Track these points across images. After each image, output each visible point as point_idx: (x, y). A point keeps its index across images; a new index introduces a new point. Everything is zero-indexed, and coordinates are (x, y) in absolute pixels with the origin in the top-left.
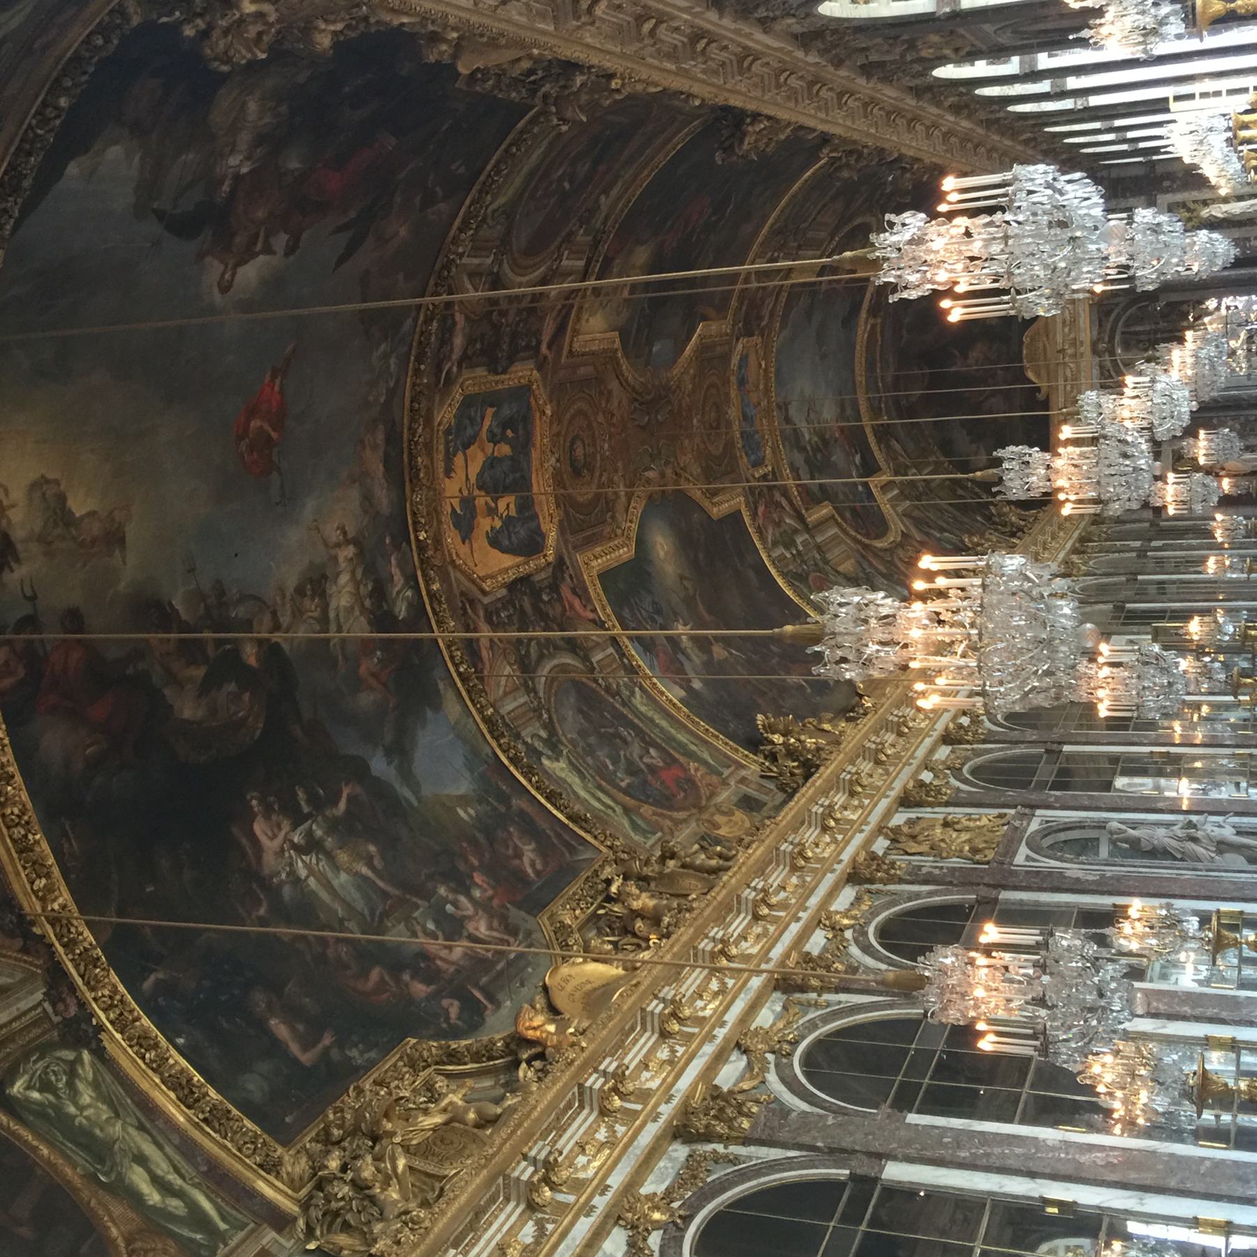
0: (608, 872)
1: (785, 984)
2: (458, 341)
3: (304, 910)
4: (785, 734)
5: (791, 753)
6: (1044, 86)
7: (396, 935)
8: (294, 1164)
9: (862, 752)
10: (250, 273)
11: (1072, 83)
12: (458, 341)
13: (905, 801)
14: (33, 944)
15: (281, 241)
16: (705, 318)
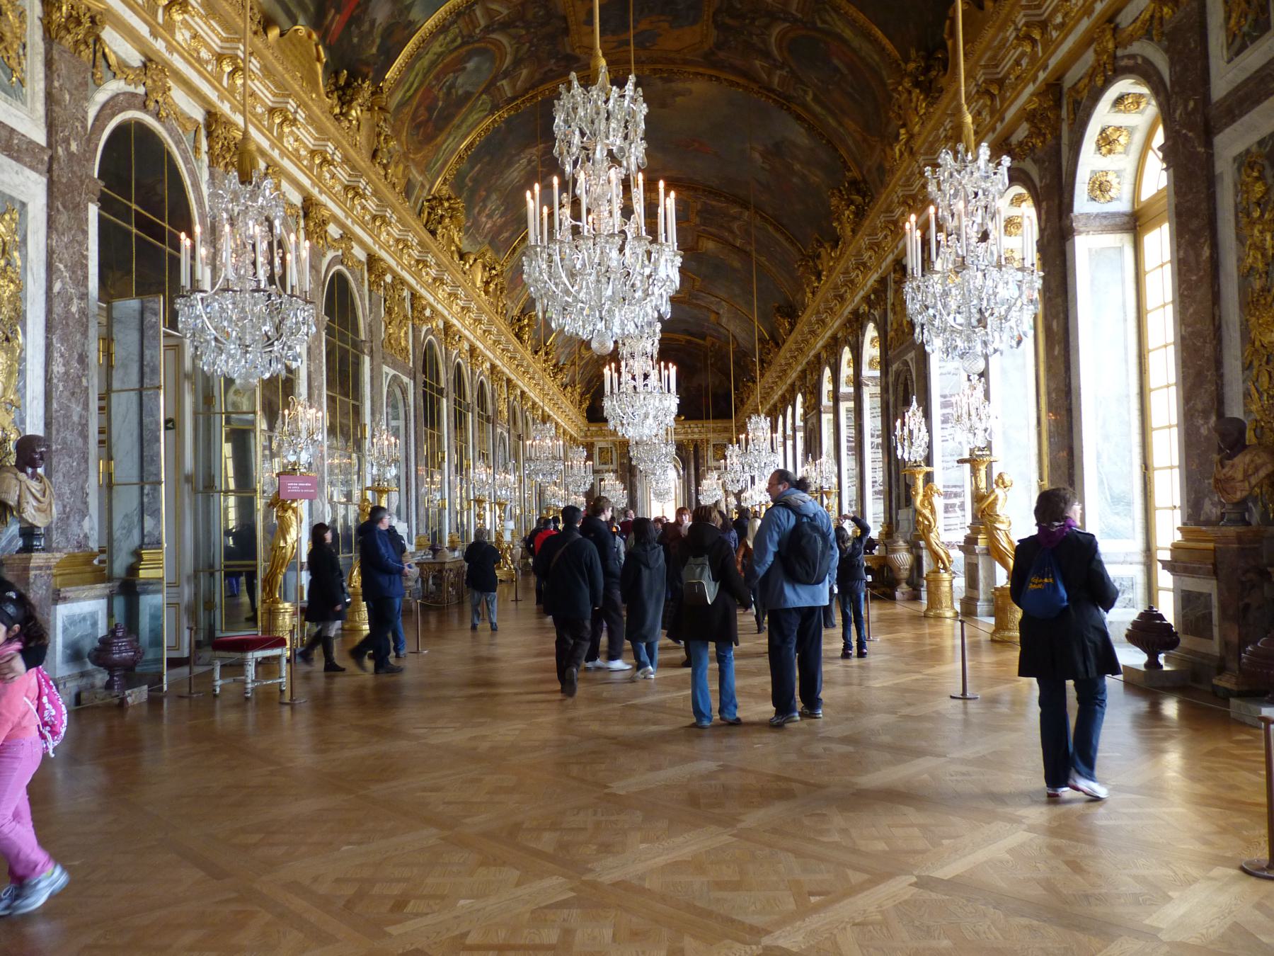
0: (498, 268)
1: (472, 350)
2: (714, 203)
3: (510, 164)
4: (528, 325)
5: (521, 328)
6: (789, 432)
7: (494, 197)
8: (445, 191)
9: (523, 359)
10: (756, 155)
11: (789, 443)
12: (714, 203)
13: (509, 381)
14: (526, 91)
15: (768, 167)
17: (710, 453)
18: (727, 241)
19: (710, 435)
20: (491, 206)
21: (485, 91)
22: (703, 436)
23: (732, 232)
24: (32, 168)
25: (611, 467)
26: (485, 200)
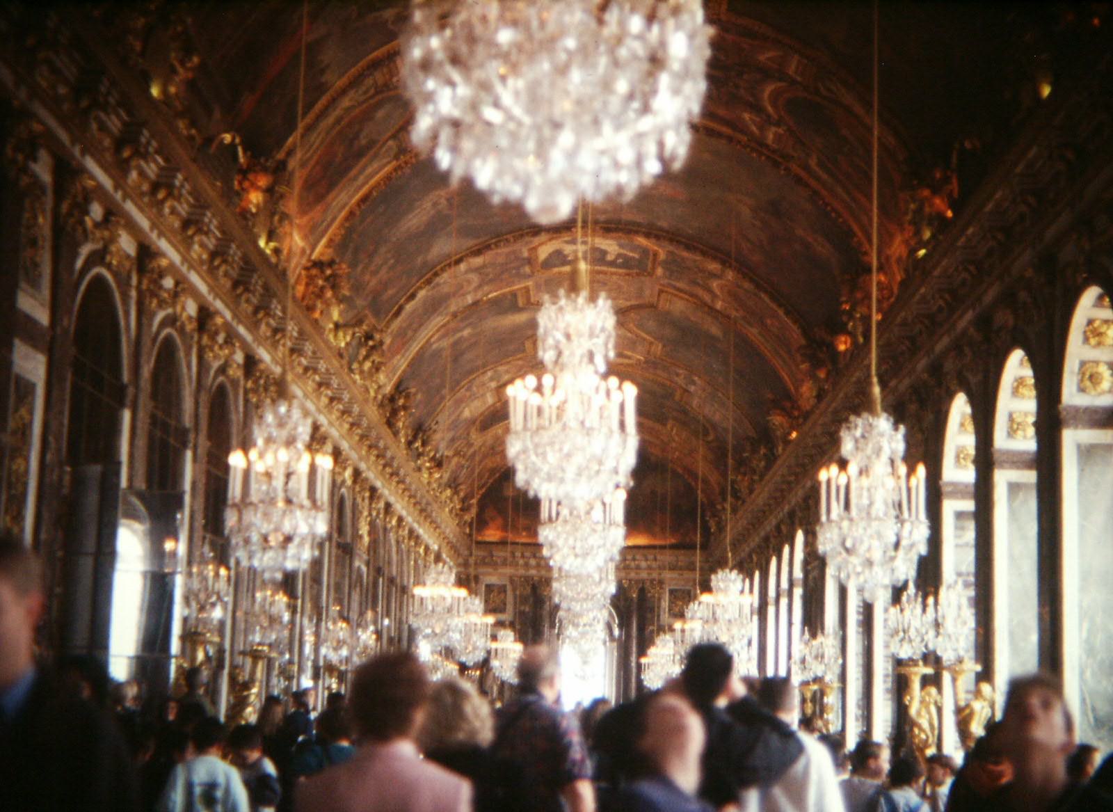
0: (377, 336)
4: (405, 408)
5: (394, 412)
6: (785, 584)
10: (746, 212)
13: (373, 490)
16: (664, 346)
17: (665, 604)
18: (705, 304)
19: (667, 575)
20: (378, 260)
21: (394, 136)
22: (655, 575)
23: (710, 291)
24: (42, 352)
25: (503, 617)
26: (371, 256)
